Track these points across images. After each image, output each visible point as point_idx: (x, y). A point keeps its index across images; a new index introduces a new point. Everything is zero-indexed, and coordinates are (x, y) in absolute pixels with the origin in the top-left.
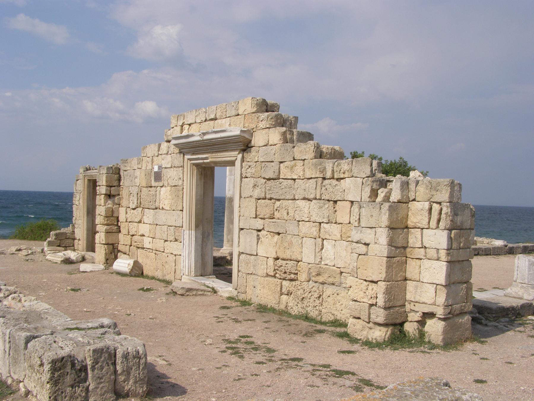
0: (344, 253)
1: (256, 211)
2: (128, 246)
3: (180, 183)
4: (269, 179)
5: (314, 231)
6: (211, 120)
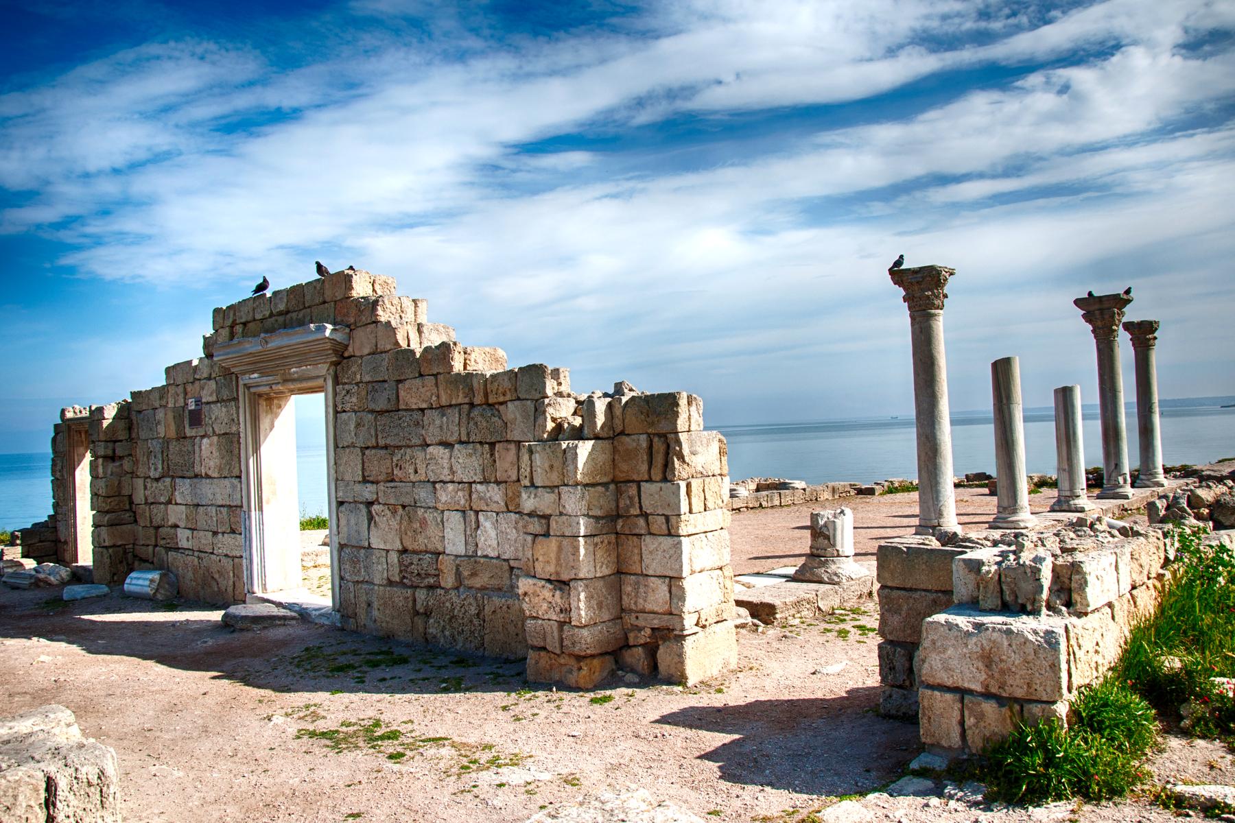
0: (513, 534)
1: (363, 469)
2: (151, 548)
3: (234, 429)
4: (381, 413)
5: (461, 498)
6: (280, 314)
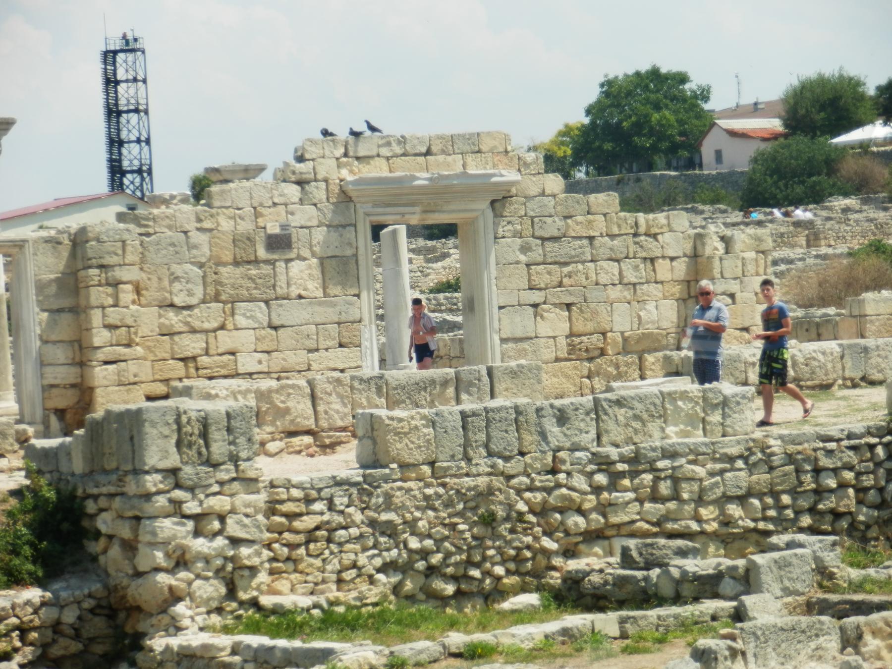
3: (349, 252)
